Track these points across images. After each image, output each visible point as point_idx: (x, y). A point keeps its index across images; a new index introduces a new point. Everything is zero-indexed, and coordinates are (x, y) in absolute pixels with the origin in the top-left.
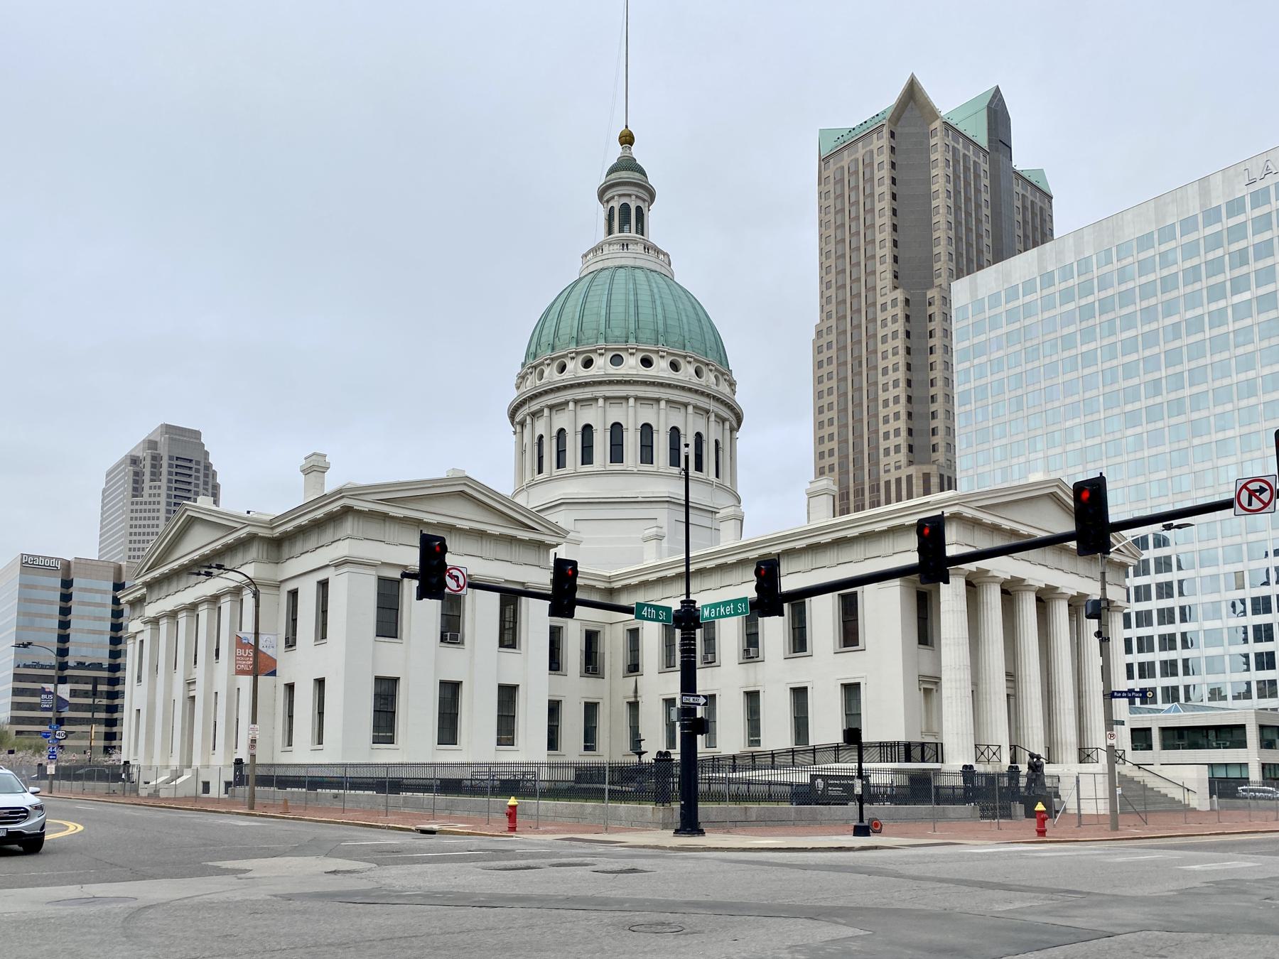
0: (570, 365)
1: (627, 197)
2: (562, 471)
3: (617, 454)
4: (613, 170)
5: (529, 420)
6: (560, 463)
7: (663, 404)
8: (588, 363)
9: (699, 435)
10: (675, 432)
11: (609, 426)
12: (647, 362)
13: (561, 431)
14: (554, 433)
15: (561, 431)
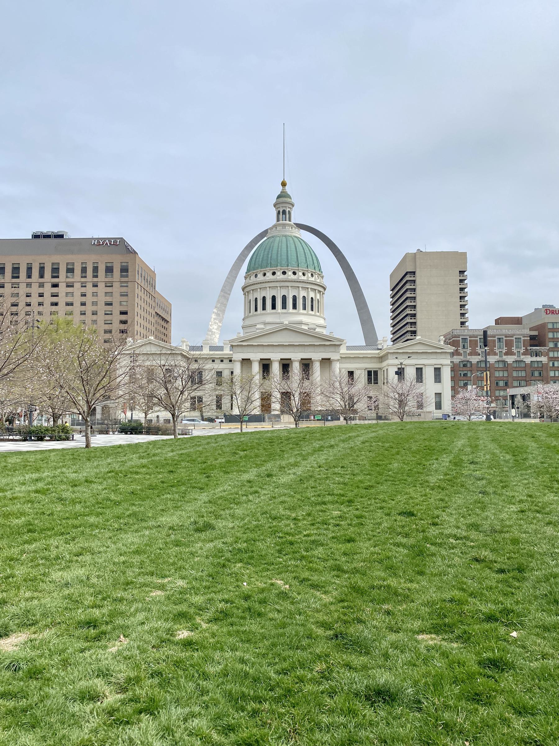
0: (259, 276)
1: (283, 206)
2: (256, 313)
3: (274, 307)
4: (279, 197)
5: (247, 294)
6: (256, 310)
7: (290, 288)
8: (265, 275)
9: (304, 297)
10: (295, 298)
11: (271, 297)
12: (284, 273)
13: (256, 299)
14: (254, 299)
15: (256, 299)
